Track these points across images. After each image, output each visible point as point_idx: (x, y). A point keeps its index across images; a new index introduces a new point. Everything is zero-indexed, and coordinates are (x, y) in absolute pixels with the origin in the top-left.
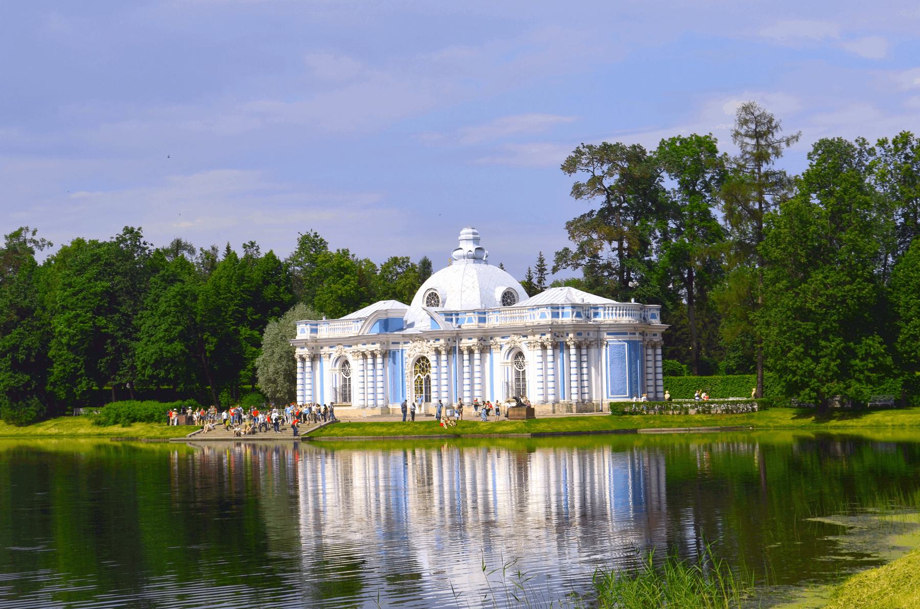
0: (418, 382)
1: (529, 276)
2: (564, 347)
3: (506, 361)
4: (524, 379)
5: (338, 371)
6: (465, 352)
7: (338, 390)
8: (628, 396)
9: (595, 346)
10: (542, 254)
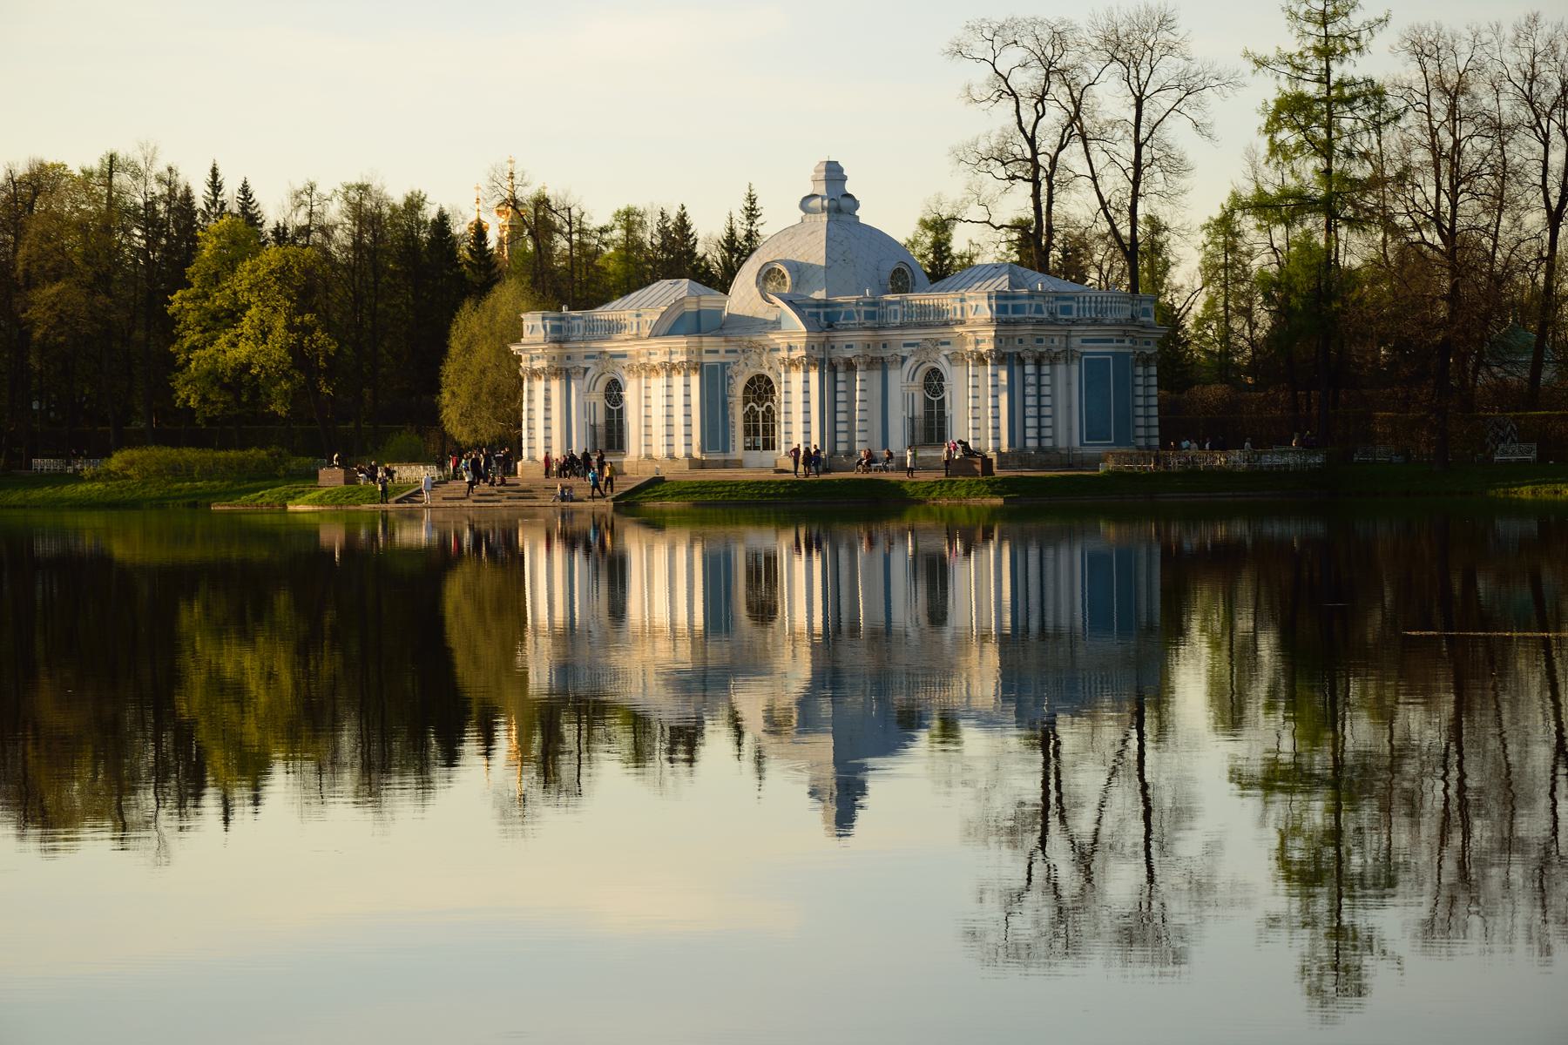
0: (750, 416)
1: (731, 229)
2: (1015, 362)
4: (942, 414)
6: (840, 368)
8: (1112, 441)
9: (1063, 361)
10: (752, 187)
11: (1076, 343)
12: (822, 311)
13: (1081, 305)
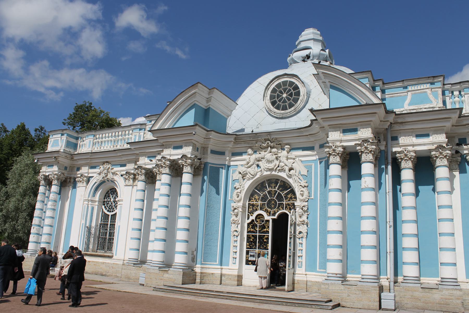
5: (97, 203)
7: (93, 231)
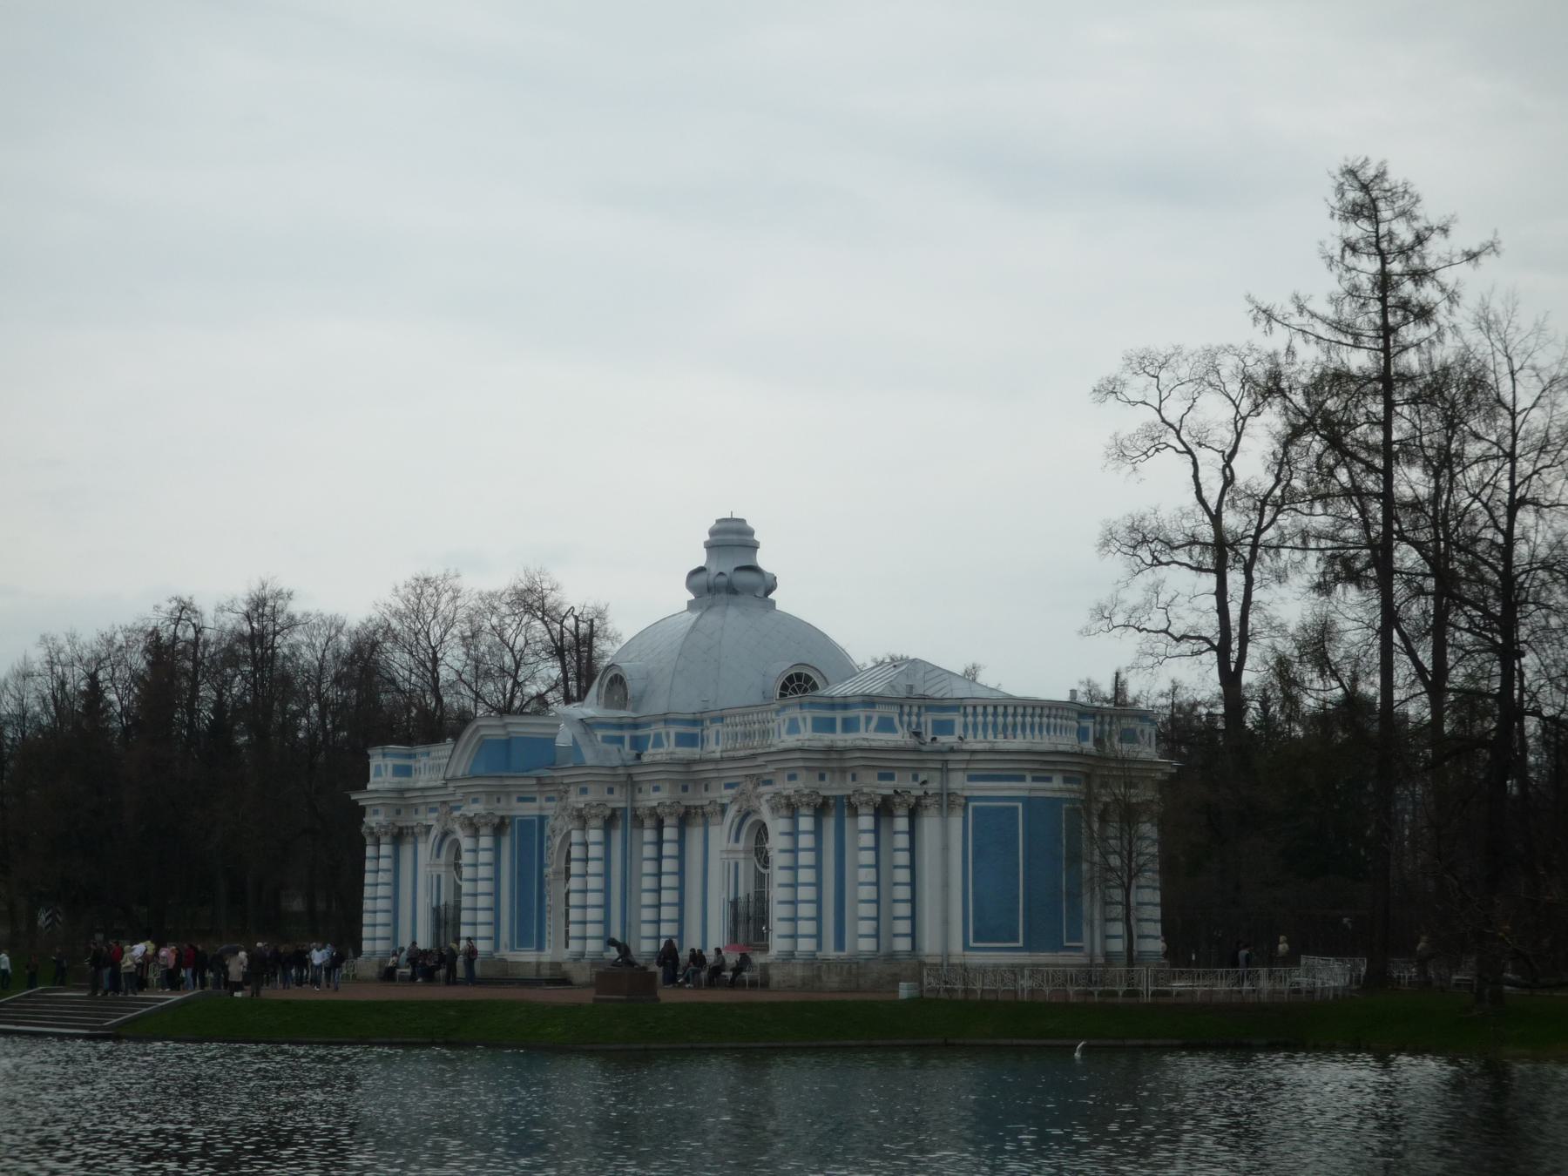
3: (732, 845)
8: (1020, 944)
11: (958, 782)
12: (627, 734)
13: (970, 719)
